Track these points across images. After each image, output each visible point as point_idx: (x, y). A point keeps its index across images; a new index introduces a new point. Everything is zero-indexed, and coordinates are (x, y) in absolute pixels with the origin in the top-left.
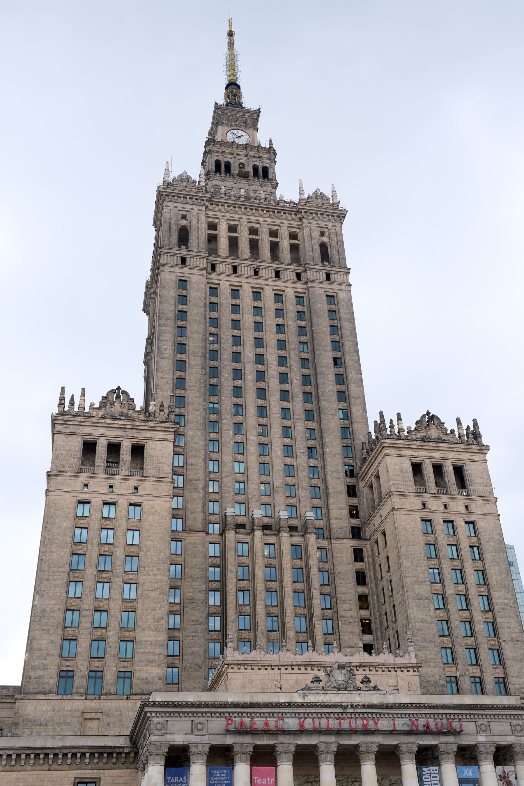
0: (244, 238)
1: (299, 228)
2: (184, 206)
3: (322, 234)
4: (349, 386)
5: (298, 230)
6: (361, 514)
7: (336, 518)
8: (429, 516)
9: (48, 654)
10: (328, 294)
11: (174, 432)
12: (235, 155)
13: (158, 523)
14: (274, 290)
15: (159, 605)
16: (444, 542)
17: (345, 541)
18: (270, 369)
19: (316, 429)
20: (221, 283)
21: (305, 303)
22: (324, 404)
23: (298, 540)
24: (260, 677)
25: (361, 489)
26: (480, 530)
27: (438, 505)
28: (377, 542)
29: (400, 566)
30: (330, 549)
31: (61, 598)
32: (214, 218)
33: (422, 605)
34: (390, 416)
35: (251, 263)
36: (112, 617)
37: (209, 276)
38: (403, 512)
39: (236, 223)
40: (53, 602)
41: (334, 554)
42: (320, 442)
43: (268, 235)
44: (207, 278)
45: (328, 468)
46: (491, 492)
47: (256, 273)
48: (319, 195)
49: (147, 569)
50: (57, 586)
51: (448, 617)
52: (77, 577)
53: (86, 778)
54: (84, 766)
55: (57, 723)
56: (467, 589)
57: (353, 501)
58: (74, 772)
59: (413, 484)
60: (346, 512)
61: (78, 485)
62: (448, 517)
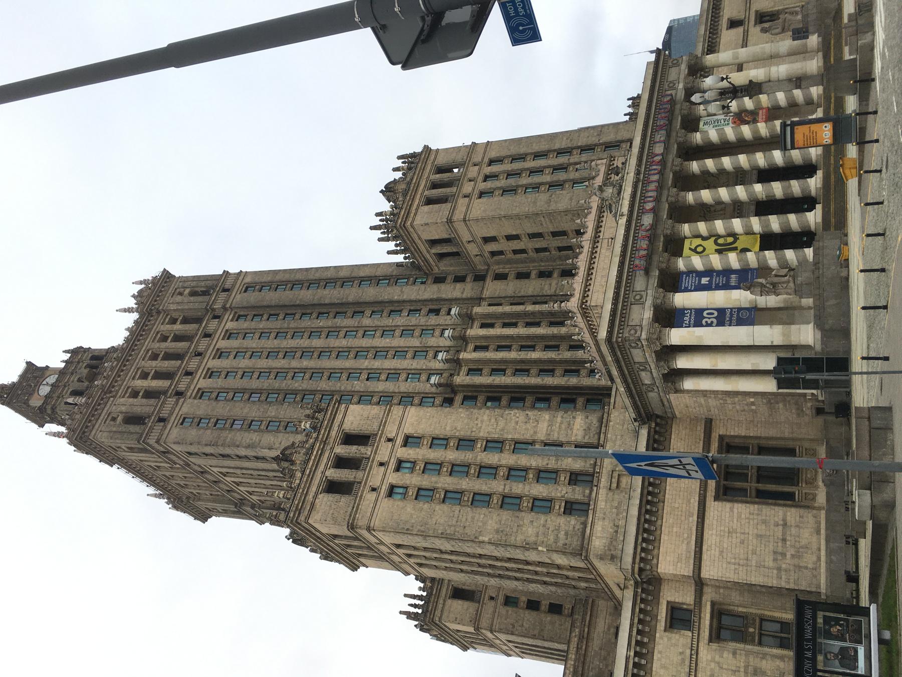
2: (101, 418)
3: (181, 294)
8: (476, 192)
9: (544, 526)
18: (303, 346)
22: (351, 299)
24: (599, 278)
28: (493, 254)
29: (518, 217)
31: (487, 513)
34: (376, 221)
39: (139, 372)
40: (490, 522)
45: (413, 297)
46: (467, 146)
47: (200, 354)
48: (139, 296)
50: (473, 518)
55: (617, 515)
57: (450, 278)
61: (371, 497)
62: (481, 178)
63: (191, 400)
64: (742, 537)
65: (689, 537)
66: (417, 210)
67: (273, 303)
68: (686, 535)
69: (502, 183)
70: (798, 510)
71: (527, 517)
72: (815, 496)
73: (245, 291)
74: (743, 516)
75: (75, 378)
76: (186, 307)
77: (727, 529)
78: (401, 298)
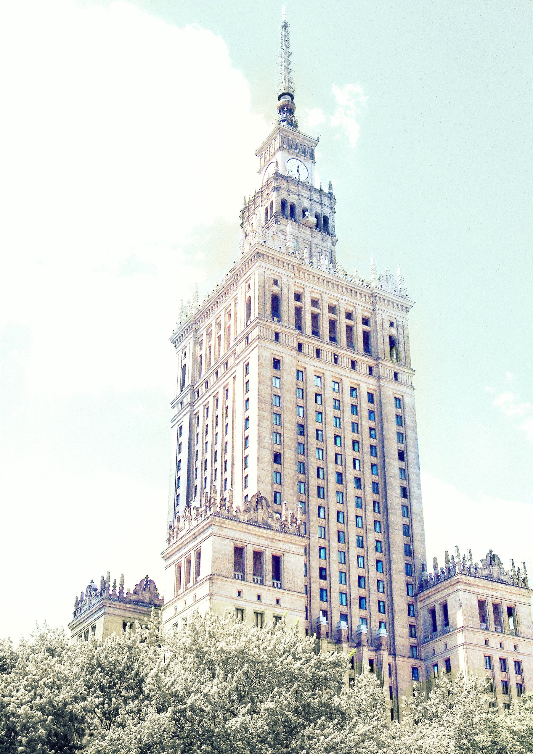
4: (412, 501)
12: (300, 197)
17: (406, 659)
18: (348, 472)
19: (383, 541)
21: (375, 402)
22: (391, 518)
25: (419, 609)
30: (394, 665)
32: (299, 287)
35: (332, 348)
41: (398, 671)
42: (387, 556)
45: (395, 585)
57: (412, 620)
60: (407, 631)
63: (295, 364)
67: (385, 433)
73: (396, 398)
75: (306, 204)
76: (379, 335)
78: (393, 572)
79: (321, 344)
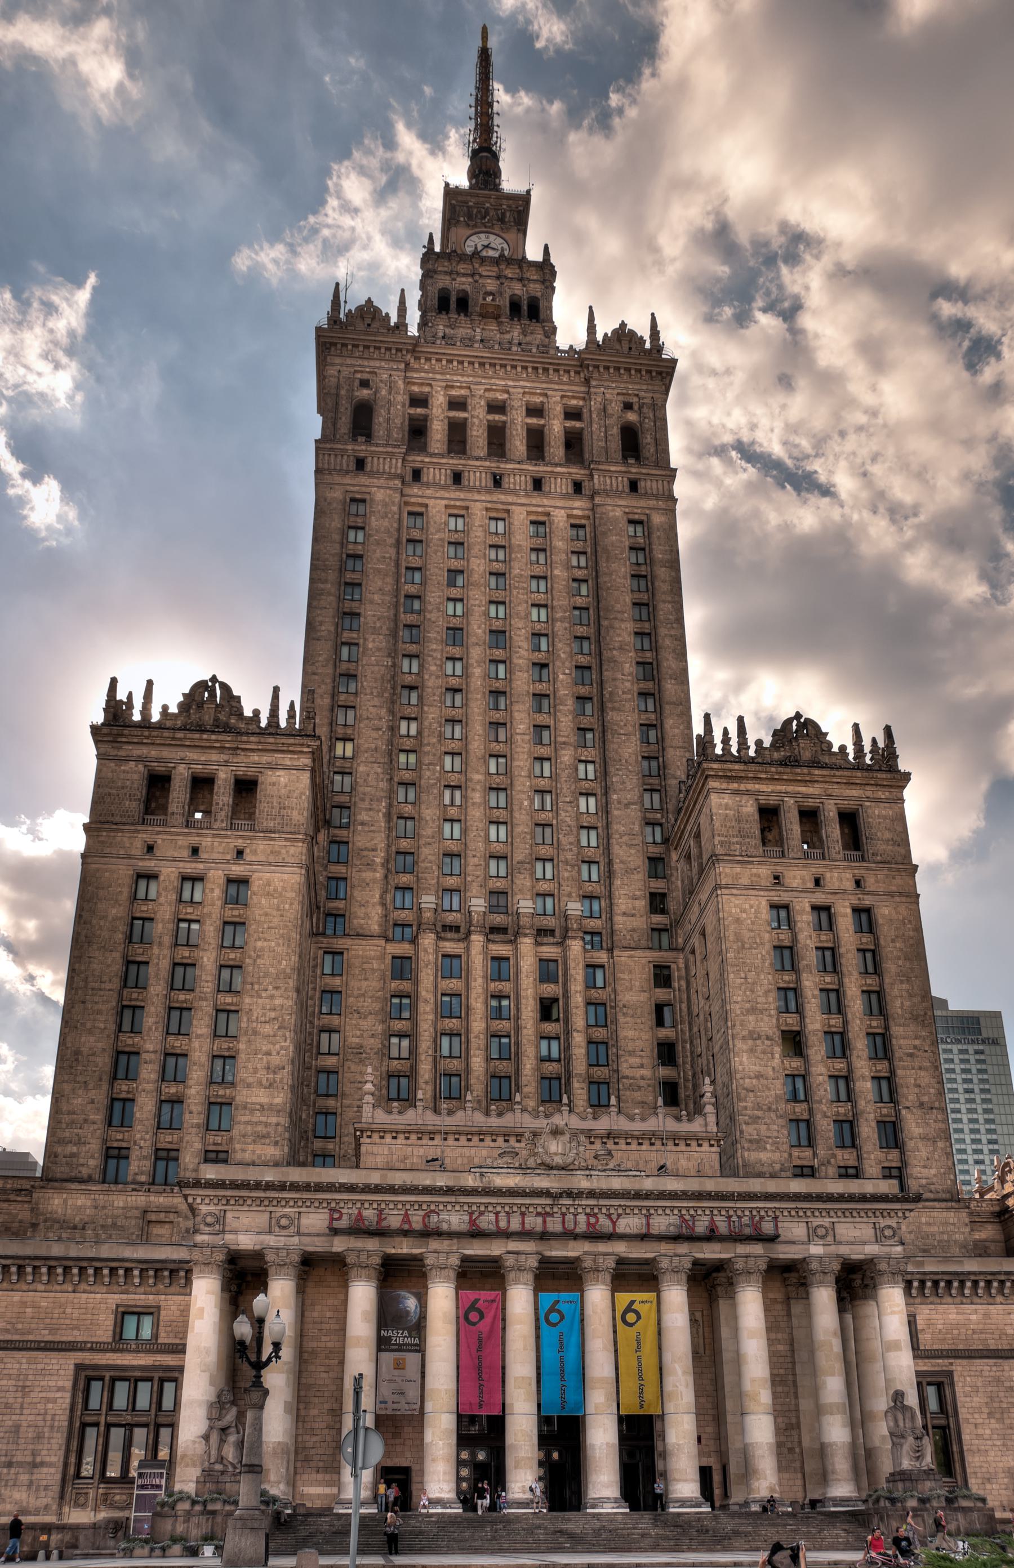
0: (478, 419)
1: (584, 399)
3: (628, 406)
5: (581, 403)
6: (672, 905)
7: (624, 914)
8: (785, 897)
9: (86, 1121)
10: (631, 517)
11: (313, 753)
12: (477, 277)
13: (278, 910)
14: (529, 513)
15: (278, 1046)
16: (808, 942)
20: (431, 502)
23: (550, 951)
26: (880, 921)
27: (803, 879)
31: (107, 1032)
32: (422, 384)
33: (759, 1049)
35: (487, 464)
36: (195, 1064)
37: (408, 491)
38: (735, 891)
39: (463, 392)
40: (92, 1039)
43: (524, 413)
44: (402, 495)
49: (256, 987)
51: (807, 1069)
52: (137, 1000)
53: (136, 1306)
54: (132, 1289)
56: (845, 1023)
58: (116, 1296)
59: (759, 842)
64: (18, 1406)
65: (17, 1331)
66: (748, 793)
68: (20, 1326)
69: (808, 938)
70: (59, 1482)
71: (100, 1095)
72: (83, 1506)
74: (50, 1406)
75: (491, 285)
77: (28, 1383)
79: (462, 462)
